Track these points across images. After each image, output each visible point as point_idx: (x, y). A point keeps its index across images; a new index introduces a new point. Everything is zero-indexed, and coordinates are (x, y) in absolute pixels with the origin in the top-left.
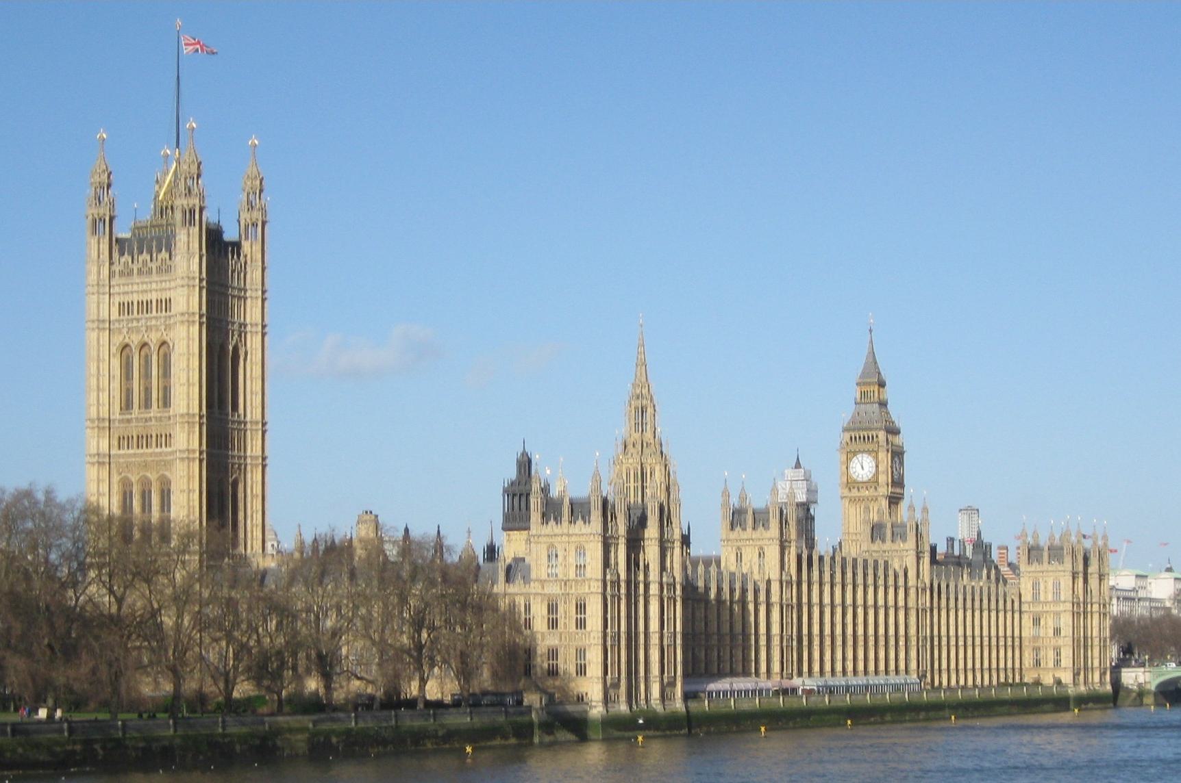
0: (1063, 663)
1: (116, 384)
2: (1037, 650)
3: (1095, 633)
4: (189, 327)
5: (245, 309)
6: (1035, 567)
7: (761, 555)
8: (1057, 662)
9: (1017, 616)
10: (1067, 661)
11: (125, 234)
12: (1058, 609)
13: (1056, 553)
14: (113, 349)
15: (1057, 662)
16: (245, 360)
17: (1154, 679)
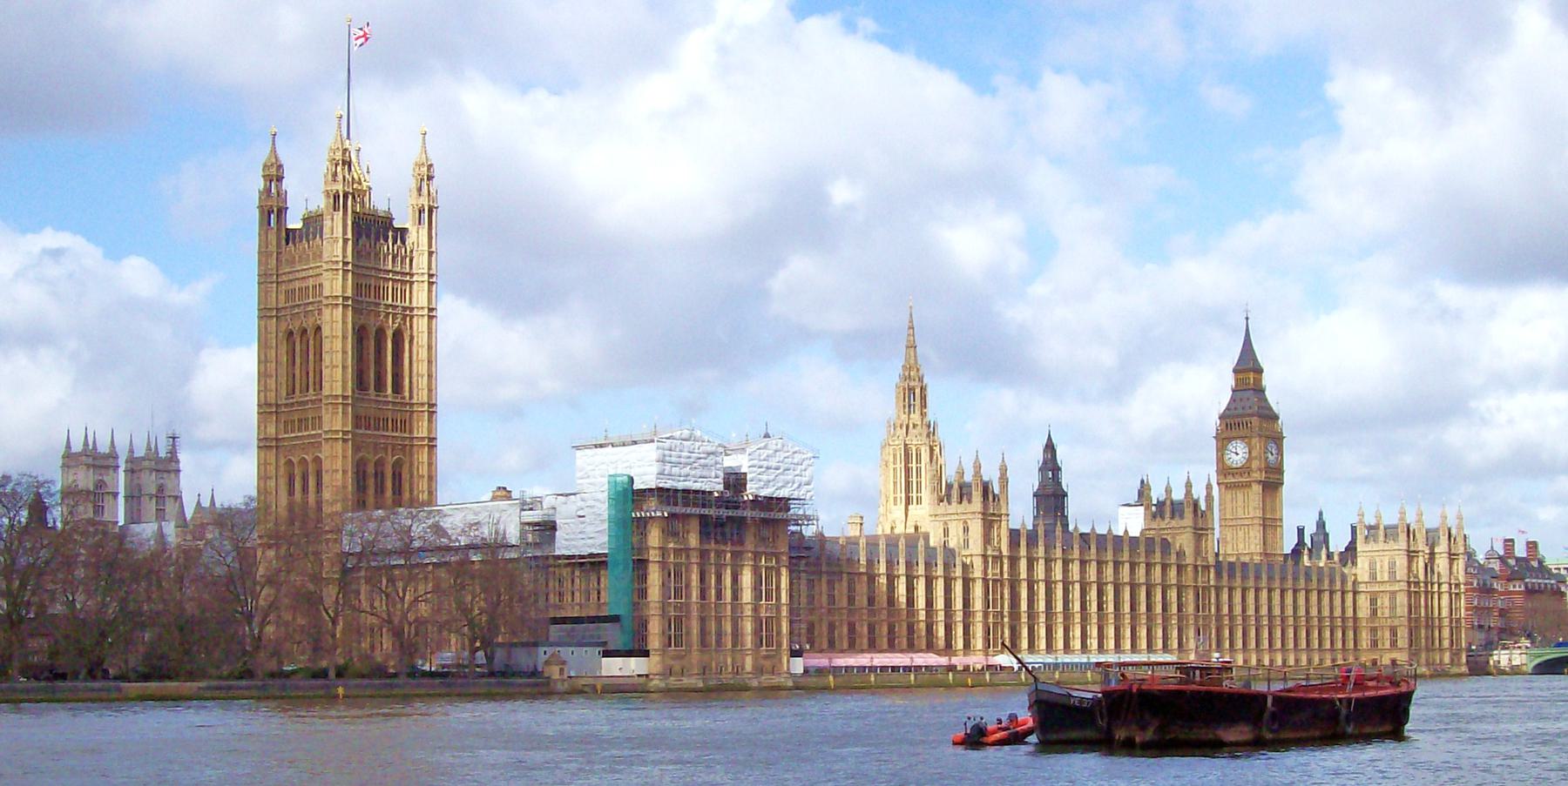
0: (1400, 644)
1: (283, 371)
2: (1374, 630)
3: (1445, 613)
4: (332, 310)
5: (411, 292)
6: (1372, 546)
7: (966, 530)
8: (1394, 644)
9: (1349, 597)
10: (1403, 642)
11: (299, 225)
12: (1392, 588)
13: (1390, 533)
14: (280, 335)
15: (1394, 644)
16: (411, 342)
17: (1531, 662)
